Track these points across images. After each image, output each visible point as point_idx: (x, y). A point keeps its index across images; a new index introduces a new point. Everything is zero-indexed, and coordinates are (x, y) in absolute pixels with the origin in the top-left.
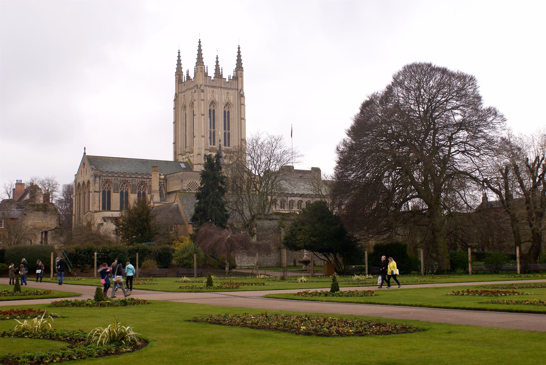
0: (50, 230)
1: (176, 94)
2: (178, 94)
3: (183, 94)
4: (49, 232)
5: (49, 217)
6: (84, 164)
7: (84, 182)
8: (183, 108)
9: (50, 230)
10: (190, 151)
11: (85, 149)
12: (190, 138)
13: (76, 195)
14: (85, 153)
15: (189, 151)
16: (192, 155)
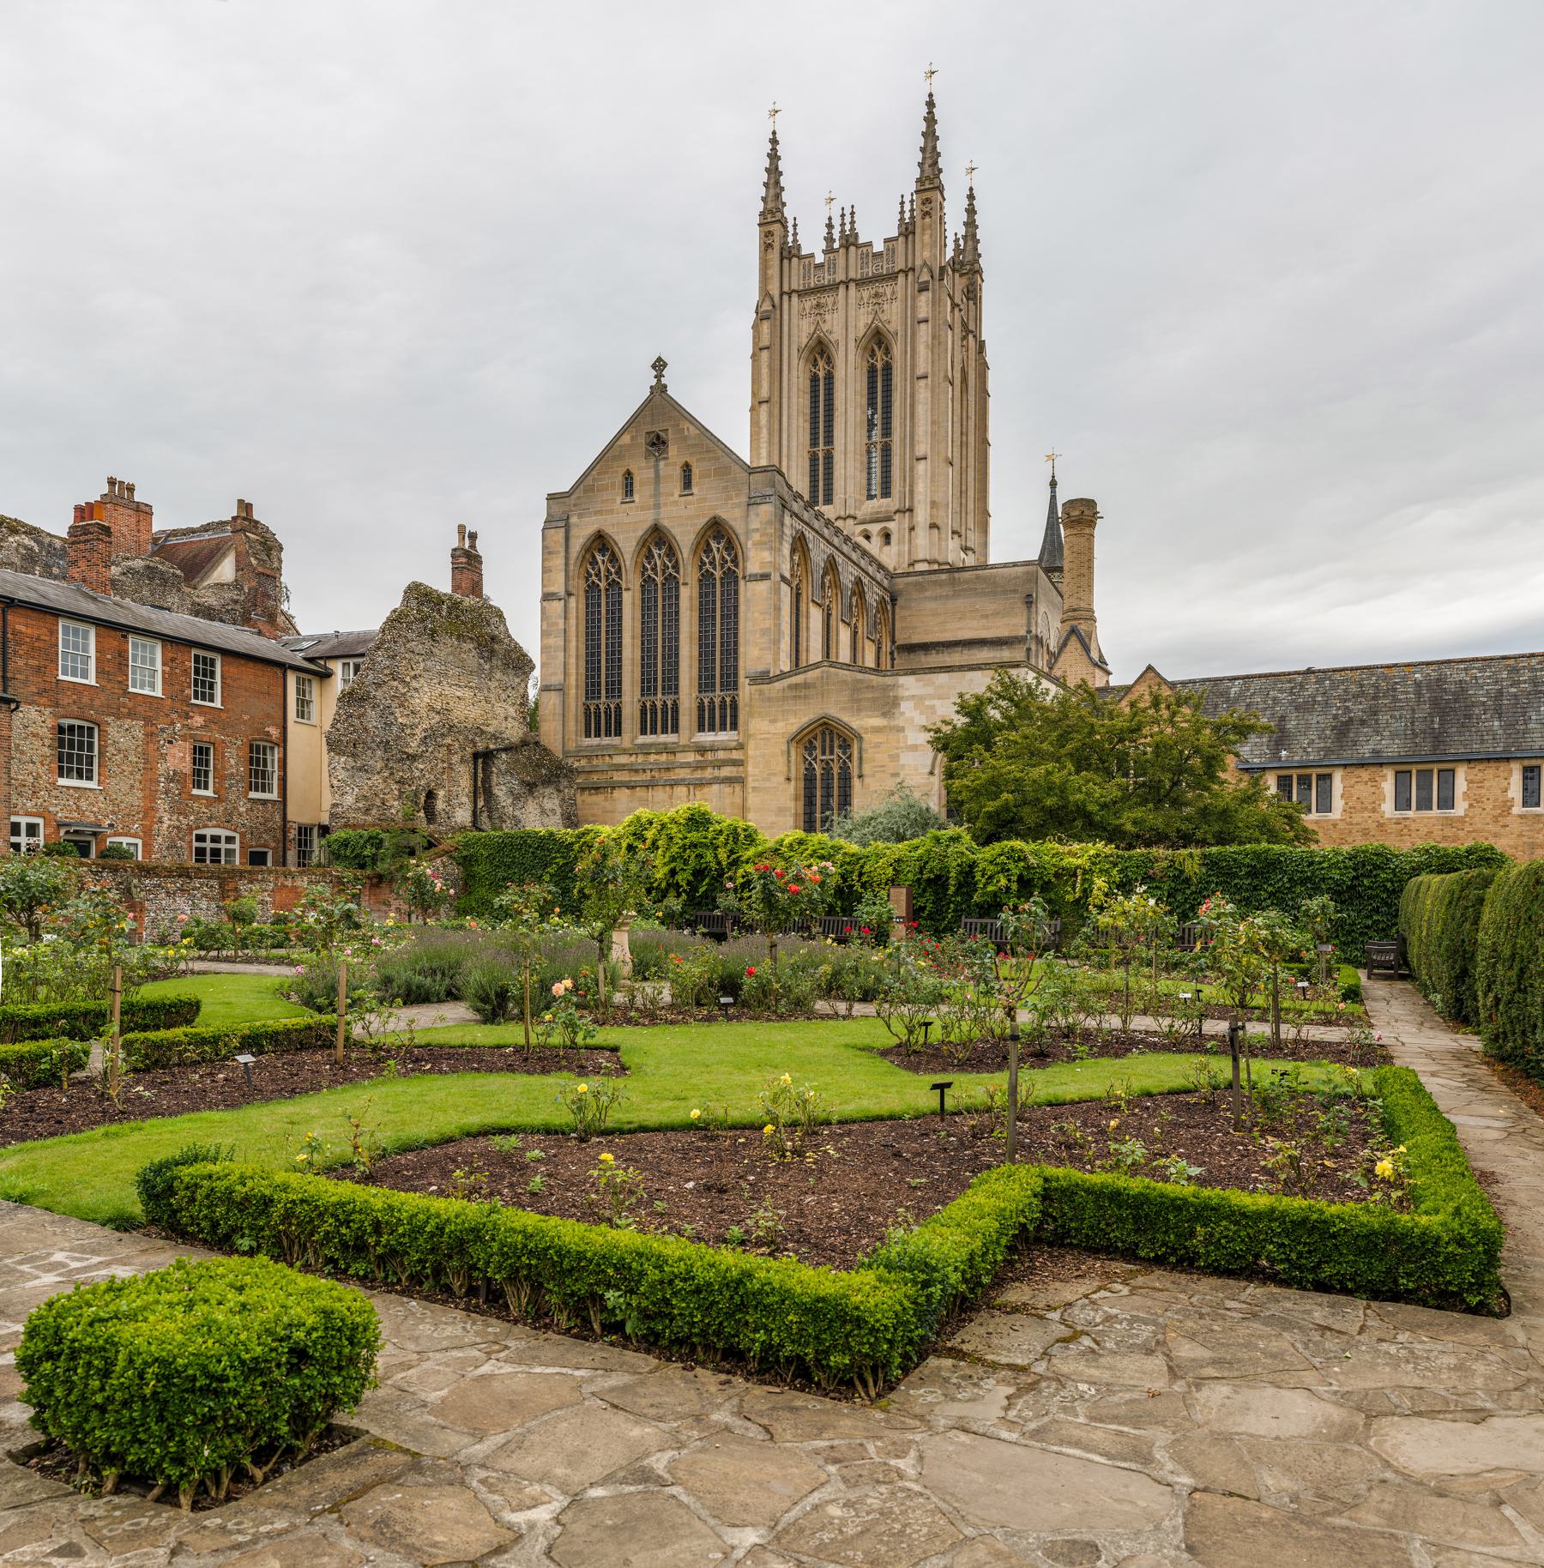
0: (505, 750)
1: (765, 294)
2: (782, 294)
3: (809, 302)
4: (504, 756)
5: (498, 675)
6: (658, 443)
7: (657, 536)
8: (805, 354)
9: (505, 750)
10: (859, 514)
11: (659, 365)
12: (858, 465)
13: (569, 594)
14: (659, 390)
15: (852, 513)
16: (875, 529)
